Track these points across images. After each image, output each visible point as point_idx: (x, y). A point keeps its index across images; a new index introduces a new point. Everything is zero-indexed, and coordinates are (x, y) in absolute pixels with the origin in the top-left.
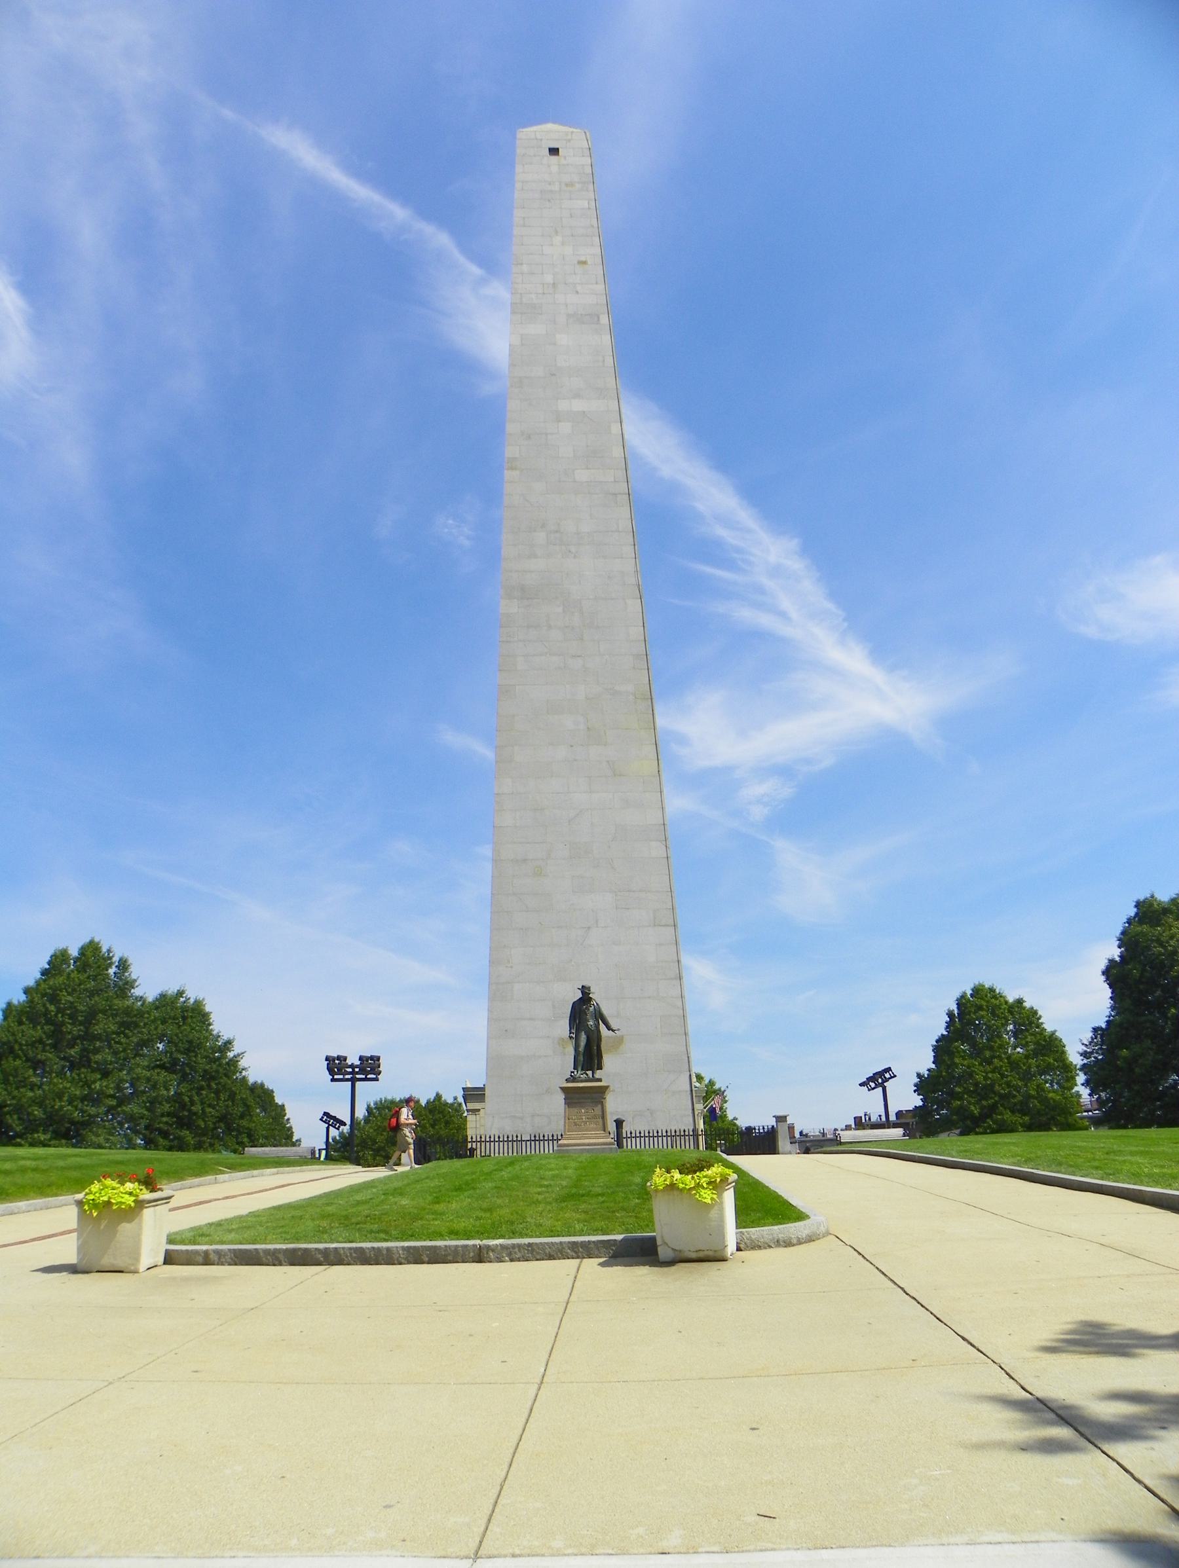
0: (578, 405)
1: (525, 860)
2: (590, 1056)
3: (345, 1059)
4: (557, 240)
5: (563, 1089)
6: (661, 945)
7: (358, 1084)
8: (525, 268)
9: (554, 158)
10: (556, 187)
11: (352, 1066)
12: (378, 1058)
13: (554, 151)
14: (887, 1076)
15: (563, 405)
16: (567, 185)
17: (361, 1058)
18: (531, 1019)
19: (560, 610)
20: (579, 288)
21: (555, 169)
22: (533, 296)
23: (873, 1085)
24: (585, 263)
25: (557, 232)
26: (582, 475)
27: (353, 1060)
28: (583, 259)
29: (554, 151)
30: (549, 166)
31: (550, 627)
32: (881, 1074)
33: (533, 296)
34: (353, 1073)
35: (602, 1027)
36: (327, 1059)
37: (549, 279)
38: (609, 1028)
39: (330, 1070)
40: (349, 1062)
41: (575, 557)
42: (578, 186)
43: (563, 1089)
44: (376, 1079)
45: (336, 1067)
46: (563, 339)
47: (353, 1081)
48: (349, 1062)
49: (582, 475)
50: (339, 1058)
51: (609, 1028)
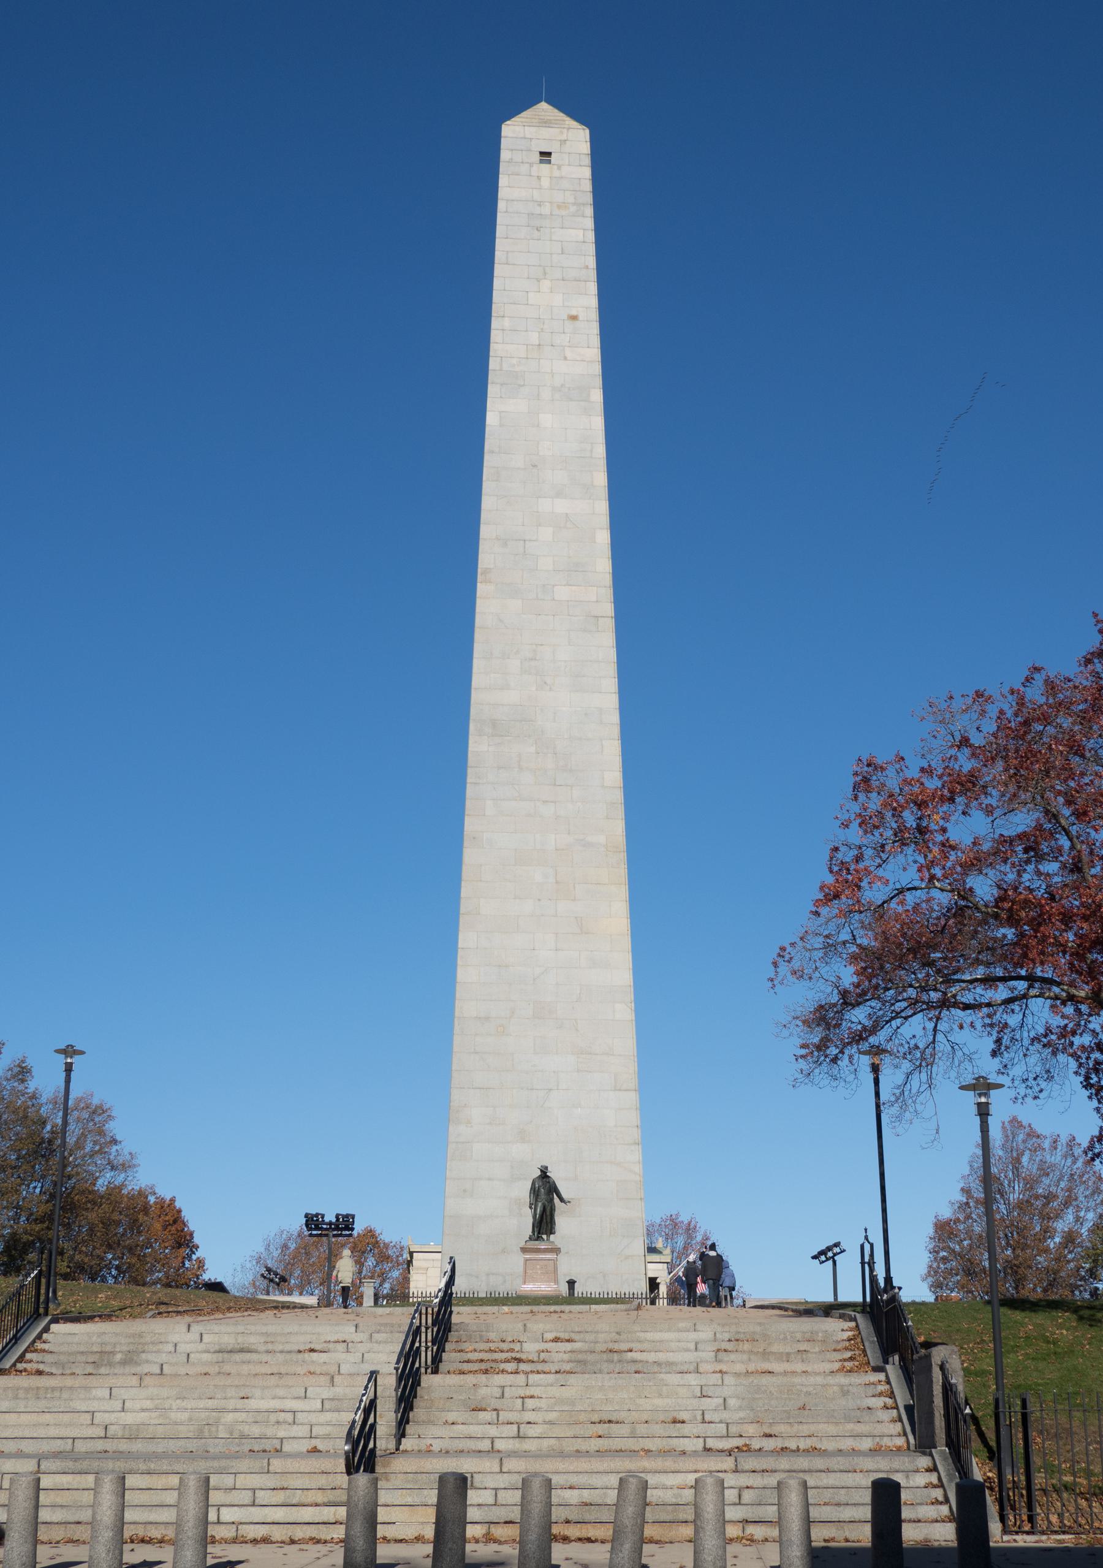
0: (561, 506)
1: (487, 1018)
3: (323, 1216)
4: (546, 284)
8: (507, 323)
10: (546, 210)
11: (330, 1223)
12: (353, 1217)
14: (837, 1250)
16: (559, 207)
18: (489, 1179)
19: (533, 749)
20: (568, 353)
21: (545, 183)
23: (823, 1258)
24: (574, 318)
25: (545, 273)
26: (563, 593)
27: (330, 1217)
28: (574, 313)
30: (539, 178)
32: (829, 1249)
33: (514, 361)
36: (306, 1216)
37: (534, 338)
40: (327, 1220)
41: (551, 689)
42: (573, 209)
46: (547, 419)
48: (327, 1220)
49: (563, 593)
50: (317, 1215)
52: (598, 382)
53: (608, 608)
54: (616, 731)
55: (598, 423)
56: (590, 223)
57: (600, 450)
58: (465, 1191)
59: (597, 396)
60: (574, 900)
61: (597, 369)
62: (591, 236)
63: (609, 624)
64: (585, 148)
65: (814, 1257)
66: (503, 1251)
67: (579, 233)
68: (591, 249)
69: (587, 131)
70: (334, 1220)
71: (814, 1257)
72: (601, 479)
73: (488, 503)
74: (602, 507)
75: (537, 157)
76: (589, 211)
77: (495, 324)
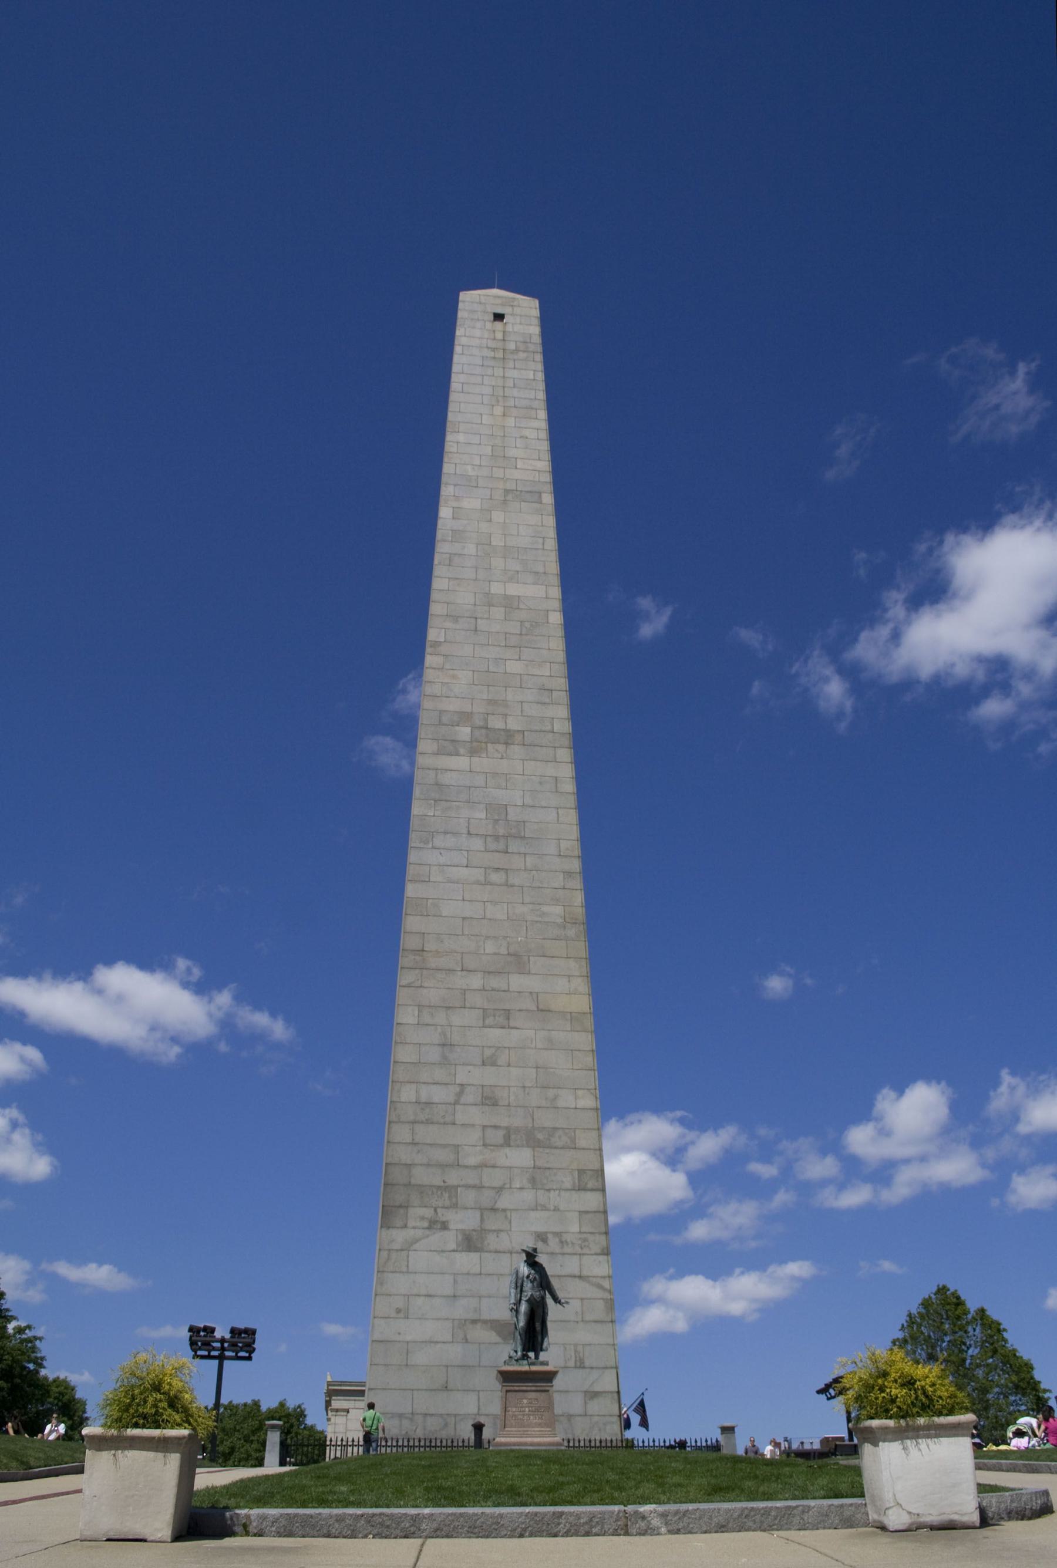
0: (513, 590)
2: (533, 1334)
3: (213, 1330)
5: (507, 1377)
6: (587, 1212)
7: (227, 1364)
8: (461, 438)
9: (498, 325)
11: (223, 1341)
13: (499, 317)
15: (496, 589)
17: (233, 1331)
19: (483, 816)
22: (469, 468)
27: (222, 1332)
29: (499, 317)
31: (469, 833)
33: (469, 468)
34: (223, 1349)
35: (549, 1301)
38: (556, 1300)
39: (193, 1343)
43: (507, 1377)
44: (249, 1358)
45: (201, 1340)
47: (221, 1358)
48: (218, 1334)
51: (556, 1300)
52: (549, 488)
53: (562, 683)
54: (572, 801)
55: (551, 521)
56: (540, 367)
57: (552, 544)
58: (398, 1311)
59: (548, 499)
60: (529, 973)
61: (547, 478)
62: (540, 376)
63: (563, 697)
64: (536, 313)
65: (819, 1392)
66: (446, 1388)
67: (530, 376)
68: (542, 386)
69: (537, 302)
70: (228, 1336)
71: (819, 1392)
72: (552, 566)
73: (439, 583)
74: (556, 592)
75: (492, 318)
76: (539, 357)
77: (449, 437)
